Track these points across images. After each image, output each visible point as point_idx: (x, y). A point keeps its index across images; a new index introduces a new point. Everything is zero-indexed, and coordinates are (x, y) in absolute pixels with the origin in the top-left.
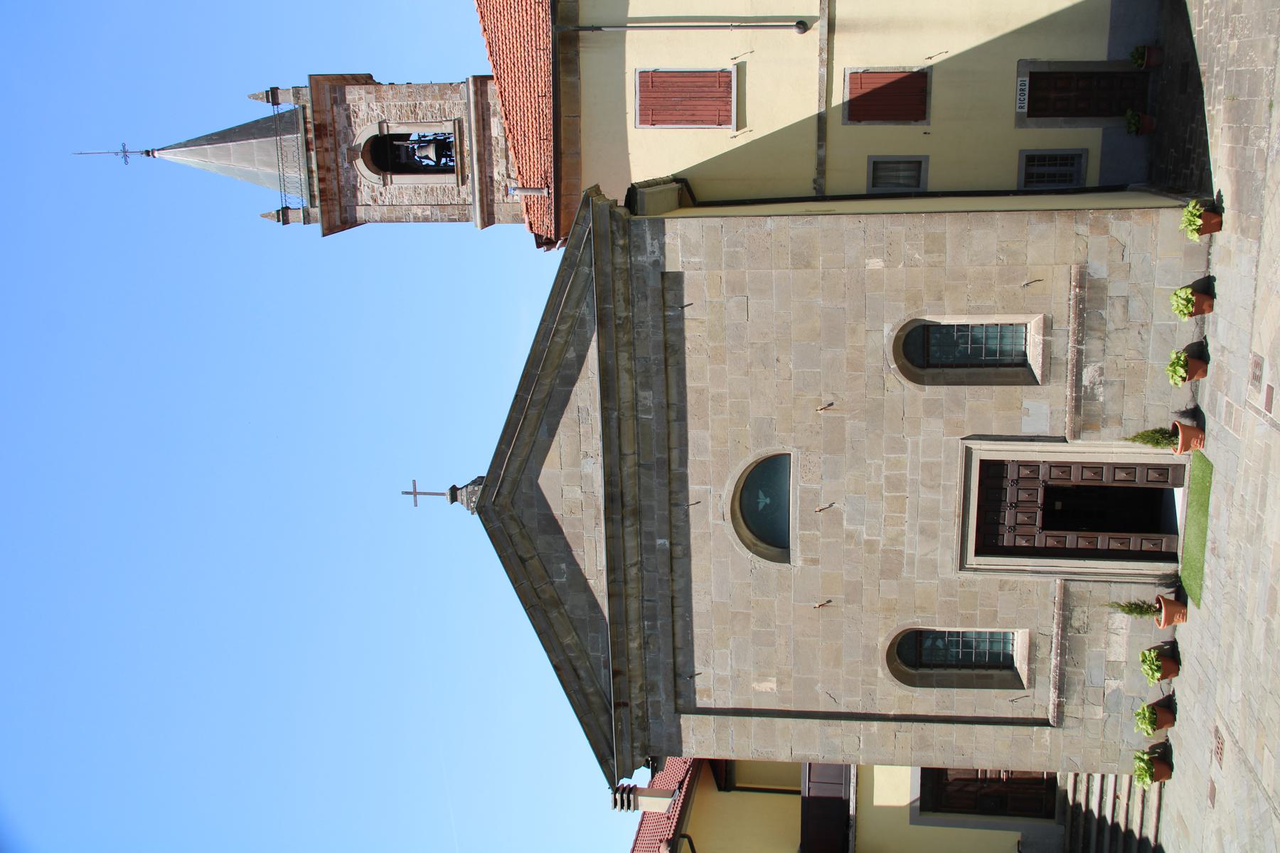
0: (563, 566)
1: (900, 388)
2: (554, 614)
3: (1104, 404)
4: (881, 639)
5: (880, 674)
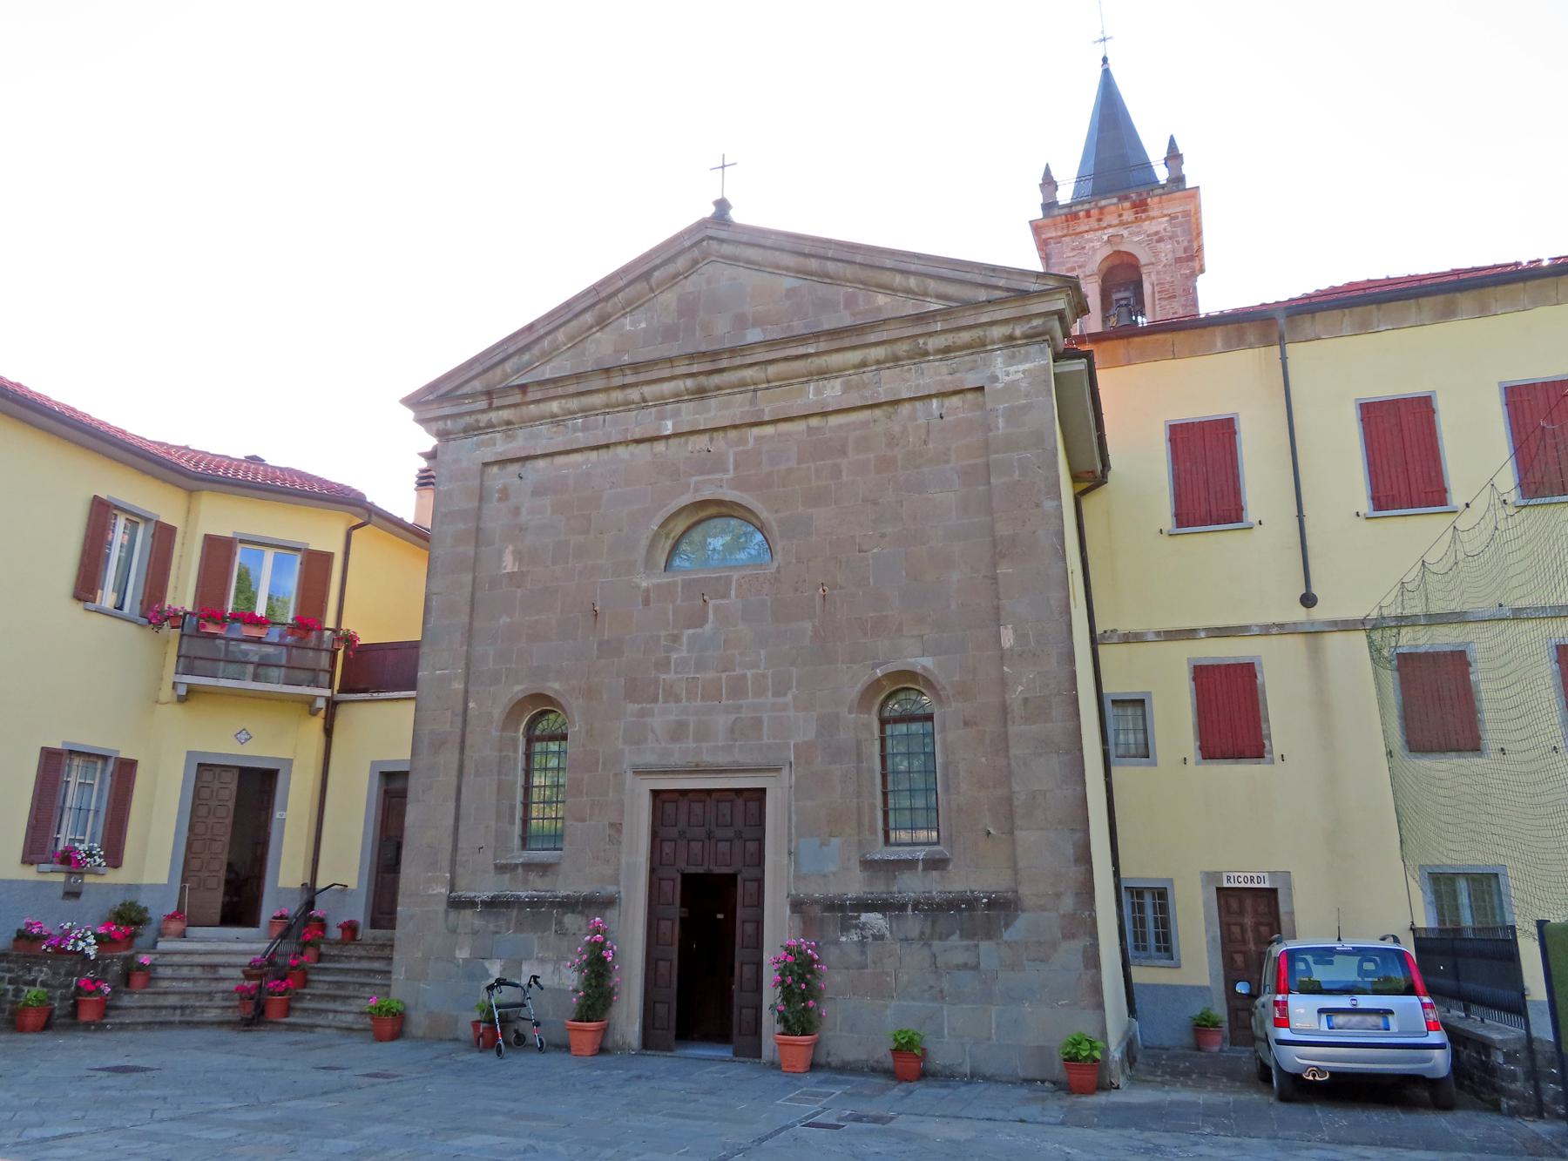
0: (643, 325)
3: (837, 943)
4: (557, 686)
5: (517, 688)
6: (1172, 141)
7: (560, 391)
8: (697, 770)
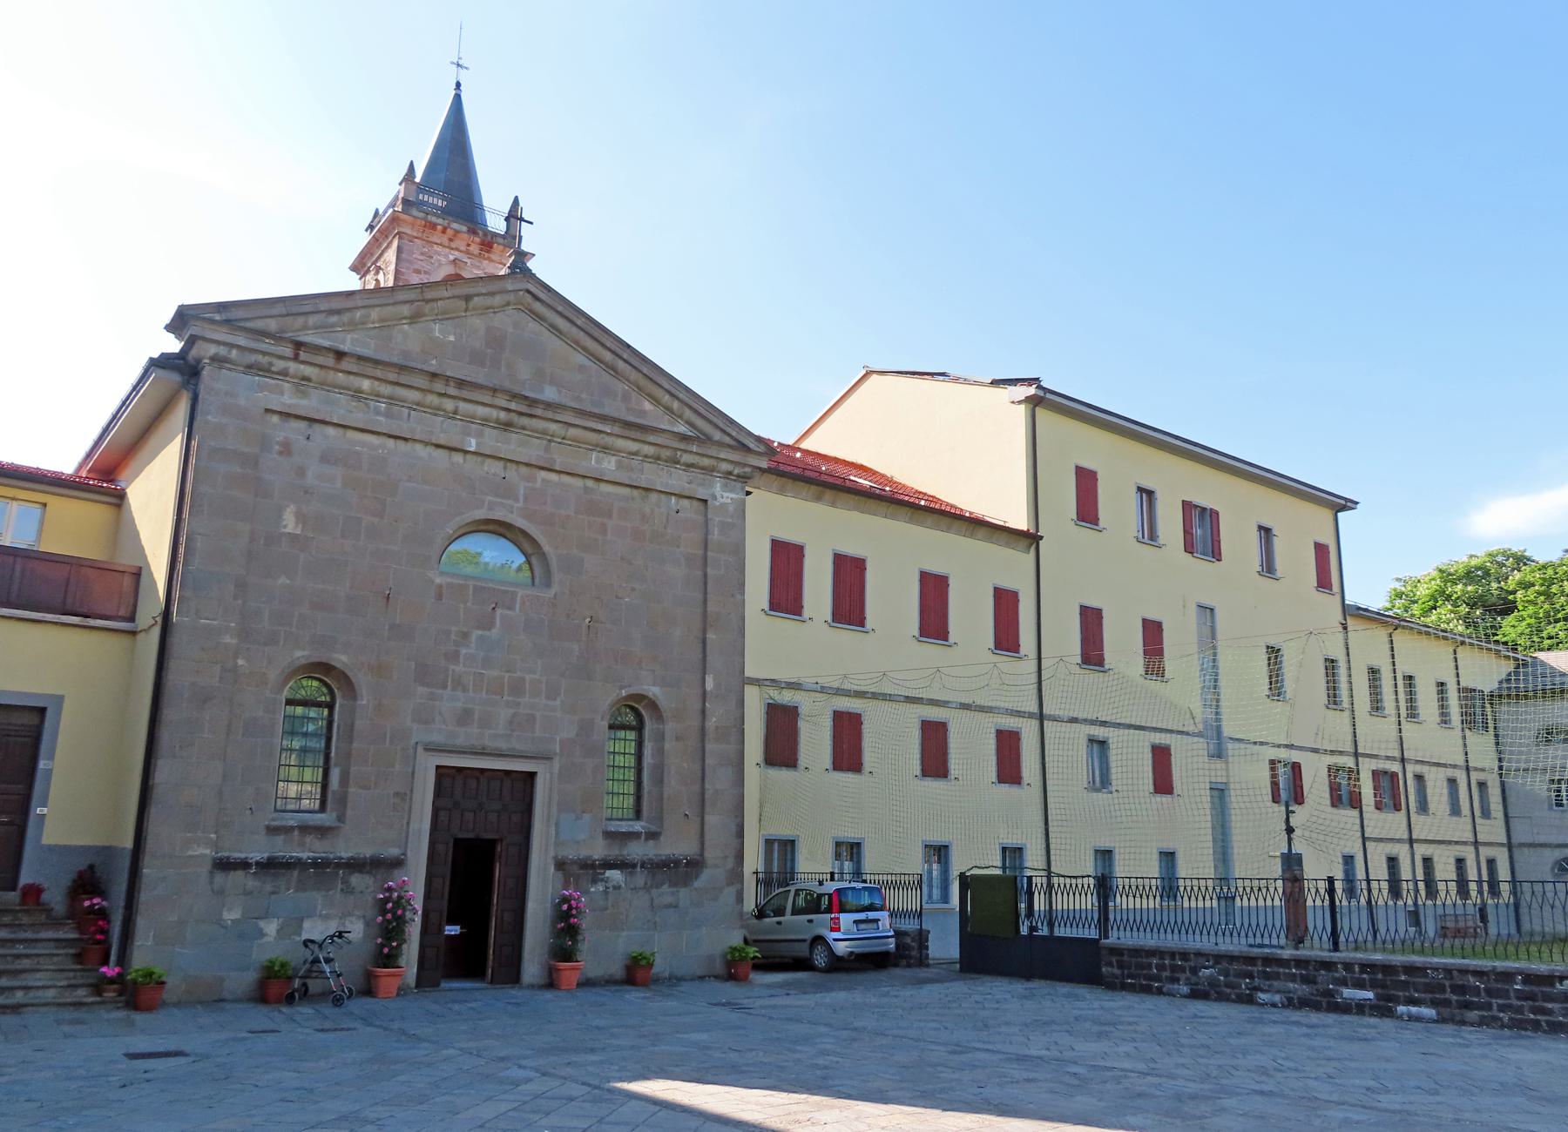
0: (452, 338)
1: (606, 697)
2: (406, 310)
3: (587, 892)
4: (344, 658)
5: (299, 653)
6: (516, 200)
7: (379, 373)
8: (500, 755)
